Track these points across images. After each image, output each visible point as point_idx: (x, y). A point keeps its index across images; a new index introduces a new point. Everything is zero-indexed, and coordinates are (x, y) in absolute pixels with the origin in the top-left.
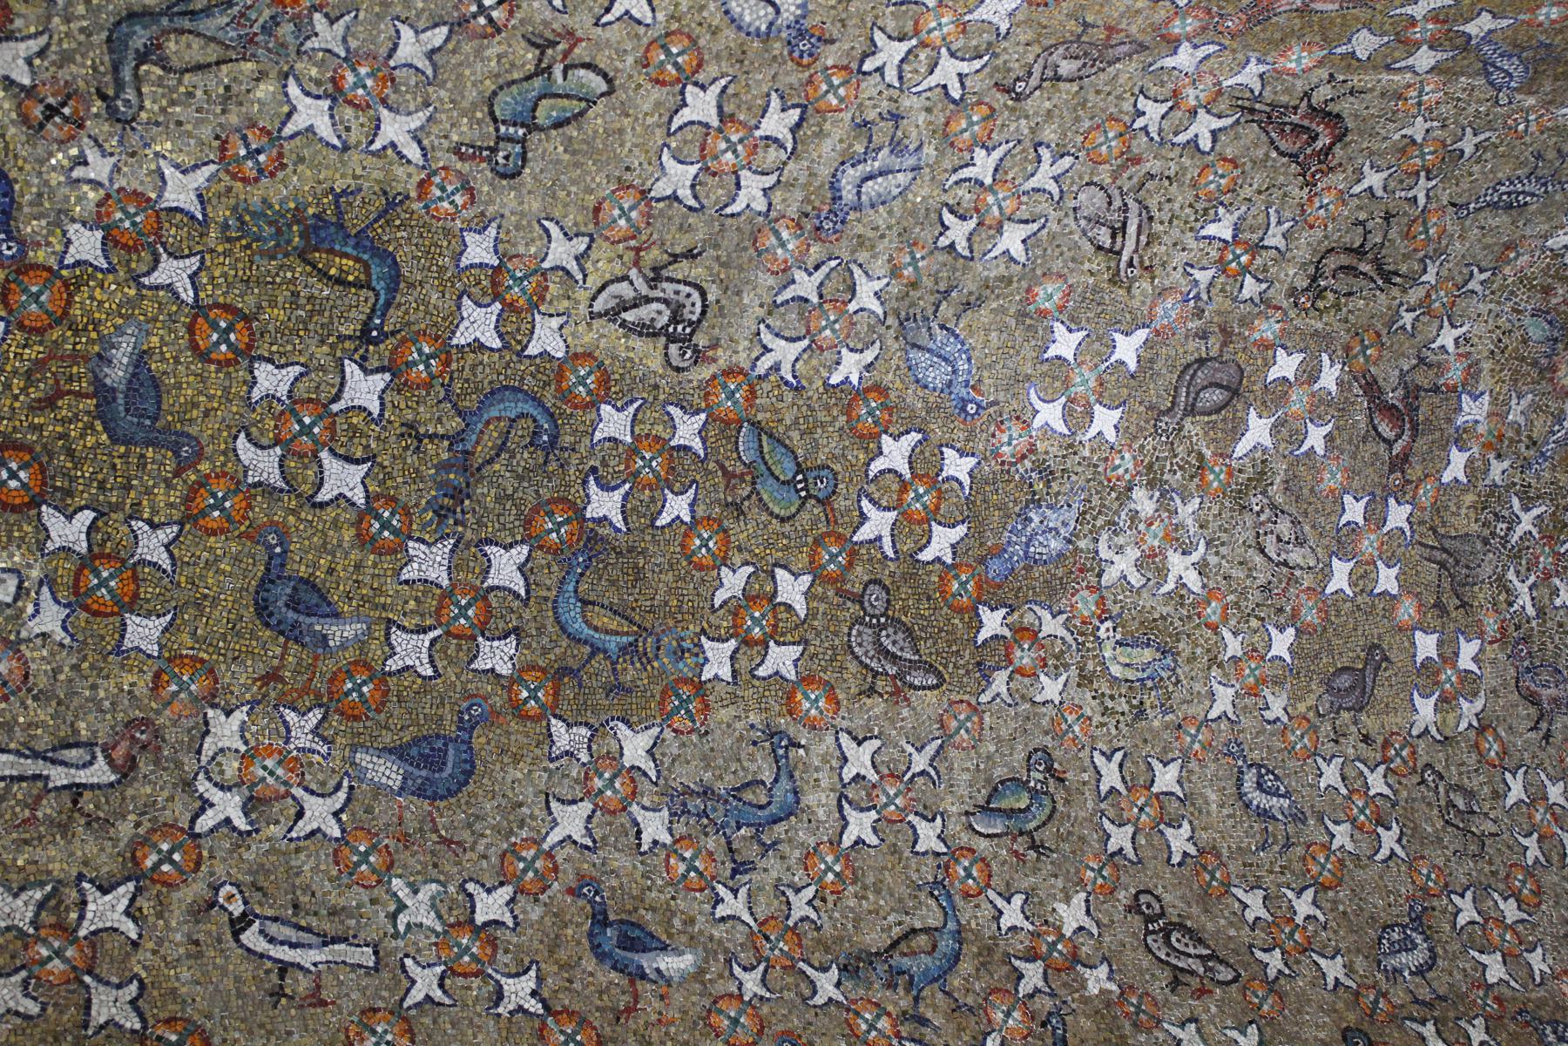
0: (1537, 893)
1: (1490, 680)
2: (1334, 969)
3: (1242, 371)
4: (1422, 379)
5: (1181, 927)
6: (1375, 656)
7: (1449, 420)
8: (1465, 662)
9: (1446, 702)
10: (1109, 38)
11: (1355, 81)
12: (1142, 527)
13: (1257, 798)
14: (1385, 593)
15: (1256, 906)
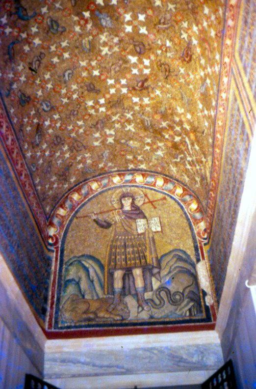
1: (99, 114)
4: (150, 89)
6: (98, 92)
9: (93, 107)
13: (67, 74)
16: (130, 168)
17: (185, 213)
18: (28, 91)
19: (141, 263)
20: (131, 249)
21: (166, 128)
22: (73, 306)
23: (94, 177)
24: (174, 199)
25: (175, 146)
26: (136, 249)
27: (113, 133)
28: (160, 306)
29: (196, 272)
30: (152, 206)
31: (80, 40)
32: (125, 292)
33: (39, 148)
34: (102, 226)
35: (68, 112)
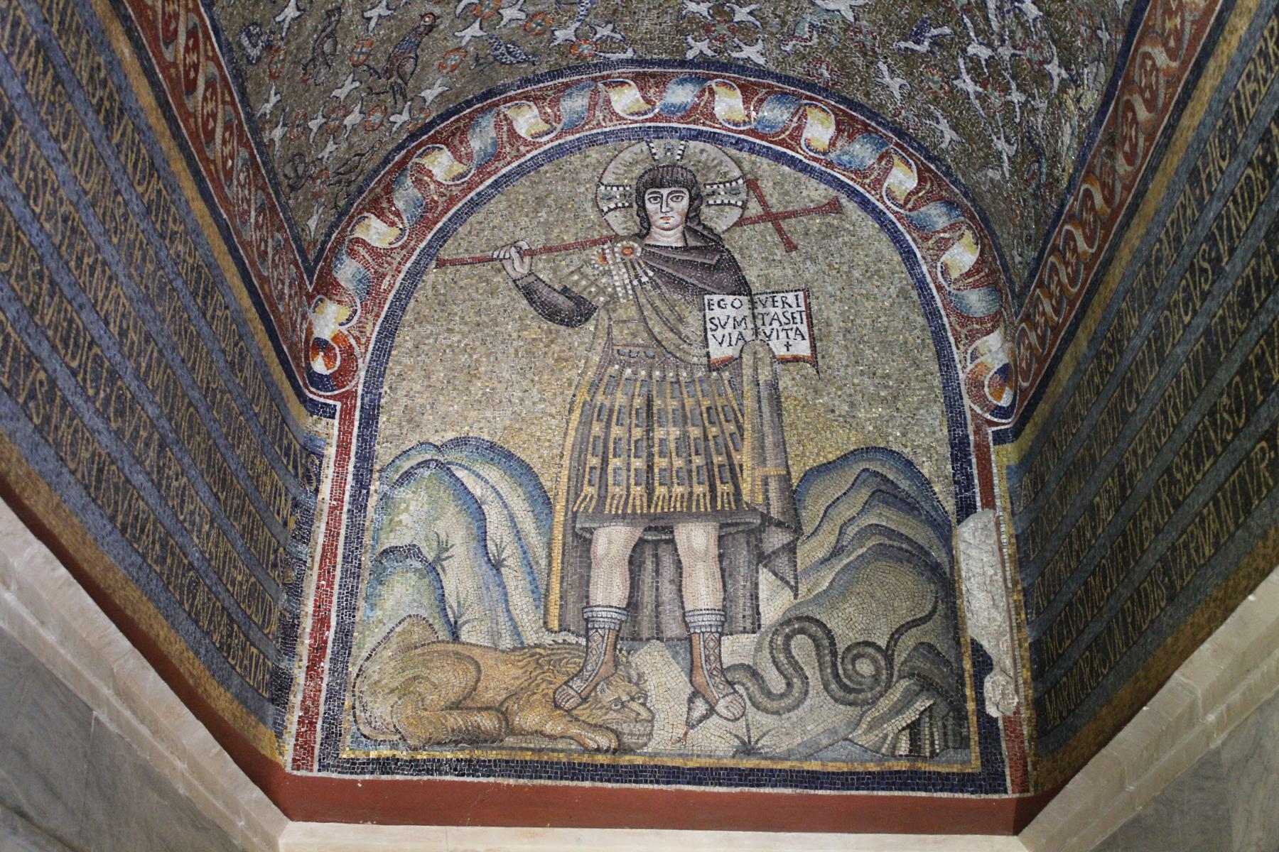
16: (690, 55)
17: (921, 285)
19: (714, 498)
20: (675, 432)
22: (409, 674)
23: (527, 81)
24: (878, 215)
26: (695, 432)
29: (953, 561)
30: (777, 239)
34: (551, 313)
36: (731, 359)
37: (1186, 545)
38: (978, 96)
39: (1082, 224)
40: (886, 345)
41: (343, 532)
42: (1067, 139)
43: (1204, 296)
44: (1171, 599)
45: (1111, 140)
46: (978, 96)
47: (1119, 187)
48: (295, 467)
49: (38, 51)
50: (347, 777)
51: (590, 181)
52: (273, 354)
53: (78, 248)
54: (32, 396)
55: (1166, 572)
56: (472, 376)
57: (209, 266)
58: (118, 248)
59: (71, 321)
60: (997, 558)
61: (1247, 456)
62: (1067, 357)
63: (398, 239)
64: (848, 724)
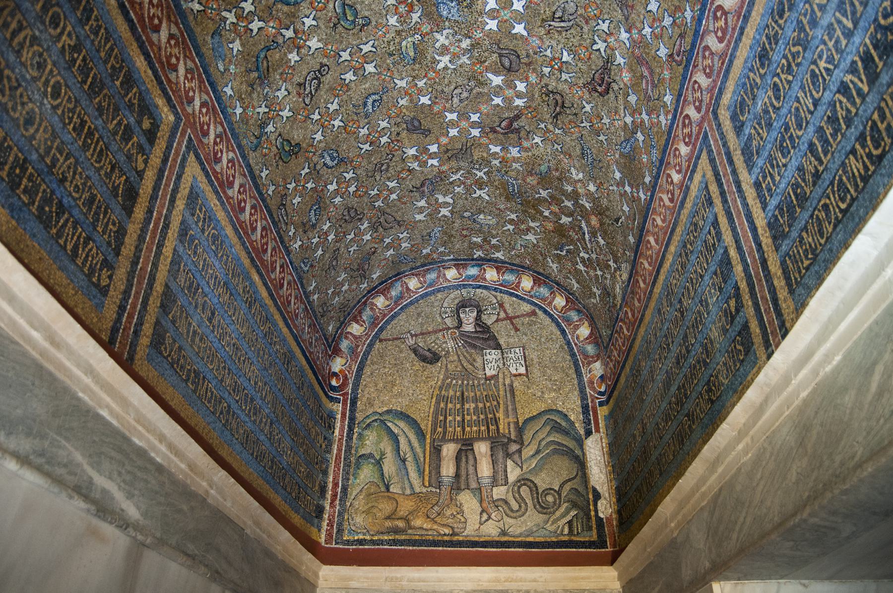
0: (360, 196)
1: (425, 170)
2: (318, 137)
3: (517, 71)
4: (523, 134)
5: (320, 83)
6: (427, 132)
7: (510, 144)
8: (430, 162)
9: (416, 158)
10: (630, 6)
11: (620, 97)
12: (457, 44)
13: (370, 101)
14: (449, 132)
15: (333, 107)
16: (475, 257)
18: (297, 136)
20: (473, 405)
21: (545, 200)
22: (370, 505)
23: (412, 269)
24: (551, 316)
25: (560, 230)
26: (481, 405)
27: (451, 201)
28: (518, 514)
29: (584, 454)
30: (511, 327)
31: (397, 41)
32: (459, 483)
33: (315, 231)
34: (424, 359)
35: (371, 167)
36: (494, 376)
37: (664, 454)
38: (585, 271)
39: (625, 323)
40: (555, 368)
41: (344, 449)
42: (618, 290)
43: (665, 358)
44: (661, 475)
45: (632, 292)
46: (585, 271)
47: (636, 312)
48: (325, 424)
49: (224, 285)
50: (346, 547)
51: (438, 306)
52: (315, 381)
53: (239, 355)
54: (221, 413)
55: (659, 464)
56: (393, 385)
57: (289, 352)
58: (254, 352)
59: (236, 382)
60: (602, 453)
61: (681, 422)
62: (623, 374)
63: (364, 332)
64: (544, 522)
